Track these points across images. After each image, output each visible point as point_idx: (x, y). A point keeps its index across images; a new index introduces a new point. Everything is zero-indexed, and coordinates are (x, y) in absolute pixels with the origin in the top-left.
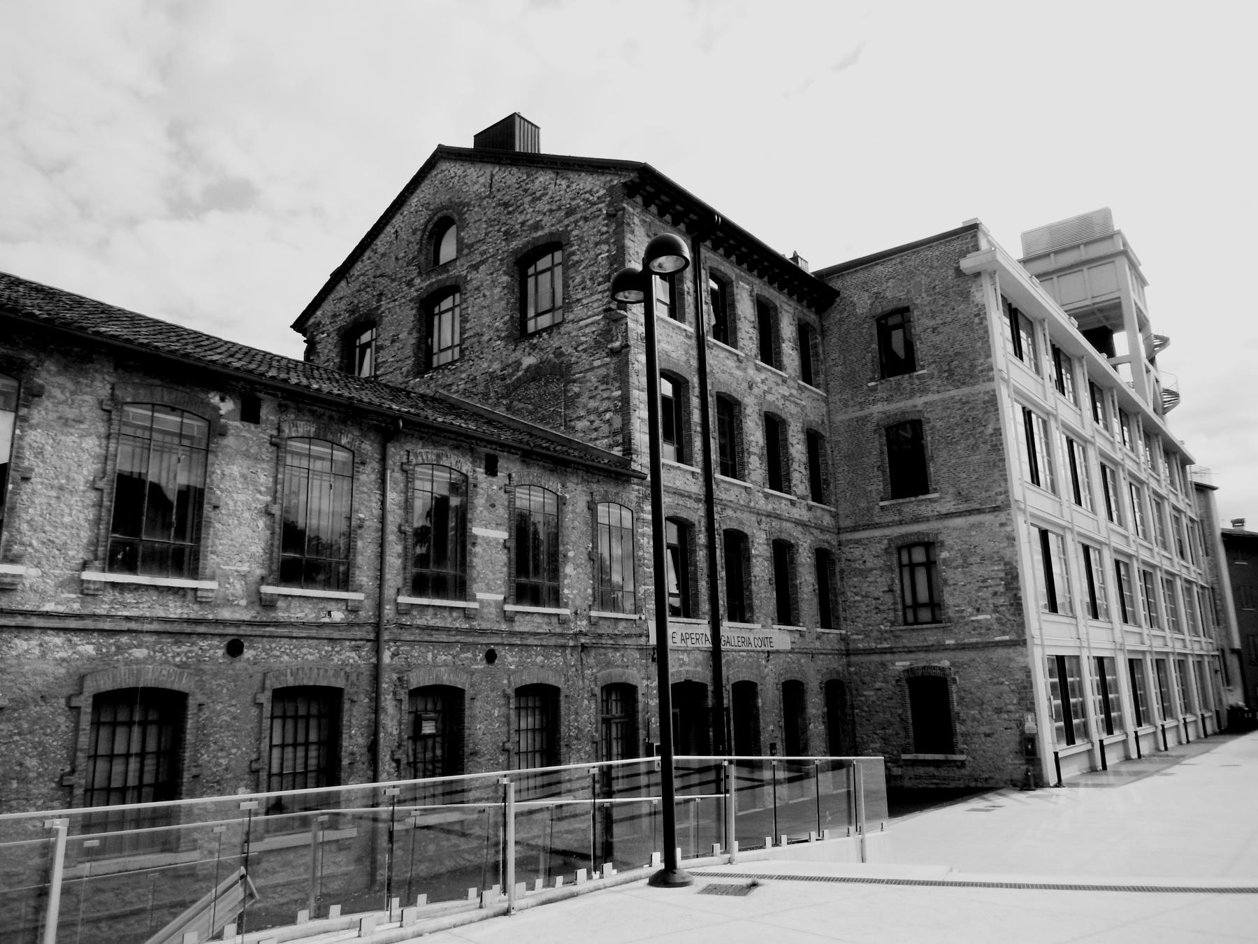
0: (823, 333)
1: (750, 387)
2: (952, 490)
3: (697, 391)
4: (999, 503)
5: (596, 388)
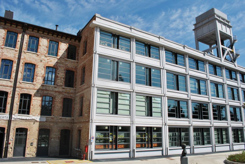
0: (79, 47)
1: (41, 61)
3: (16, 63)
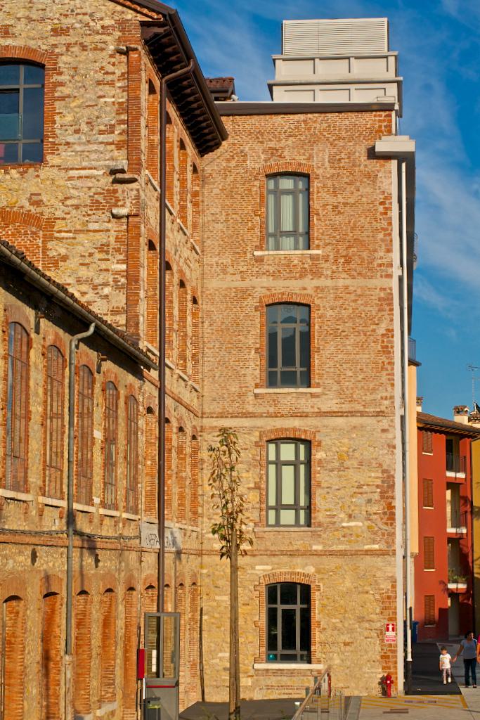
2: (335, 387)
4: (383, 408)
5: (91, 255)
